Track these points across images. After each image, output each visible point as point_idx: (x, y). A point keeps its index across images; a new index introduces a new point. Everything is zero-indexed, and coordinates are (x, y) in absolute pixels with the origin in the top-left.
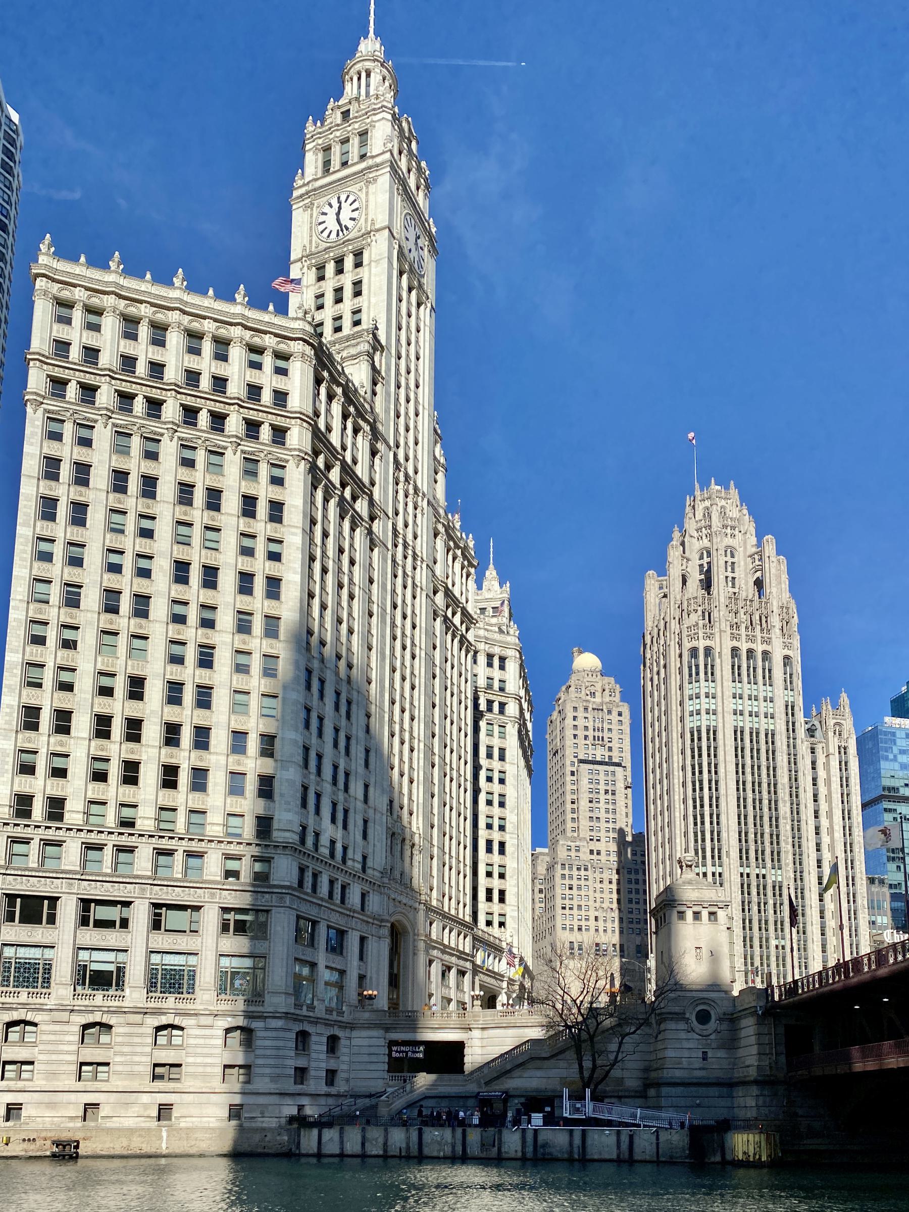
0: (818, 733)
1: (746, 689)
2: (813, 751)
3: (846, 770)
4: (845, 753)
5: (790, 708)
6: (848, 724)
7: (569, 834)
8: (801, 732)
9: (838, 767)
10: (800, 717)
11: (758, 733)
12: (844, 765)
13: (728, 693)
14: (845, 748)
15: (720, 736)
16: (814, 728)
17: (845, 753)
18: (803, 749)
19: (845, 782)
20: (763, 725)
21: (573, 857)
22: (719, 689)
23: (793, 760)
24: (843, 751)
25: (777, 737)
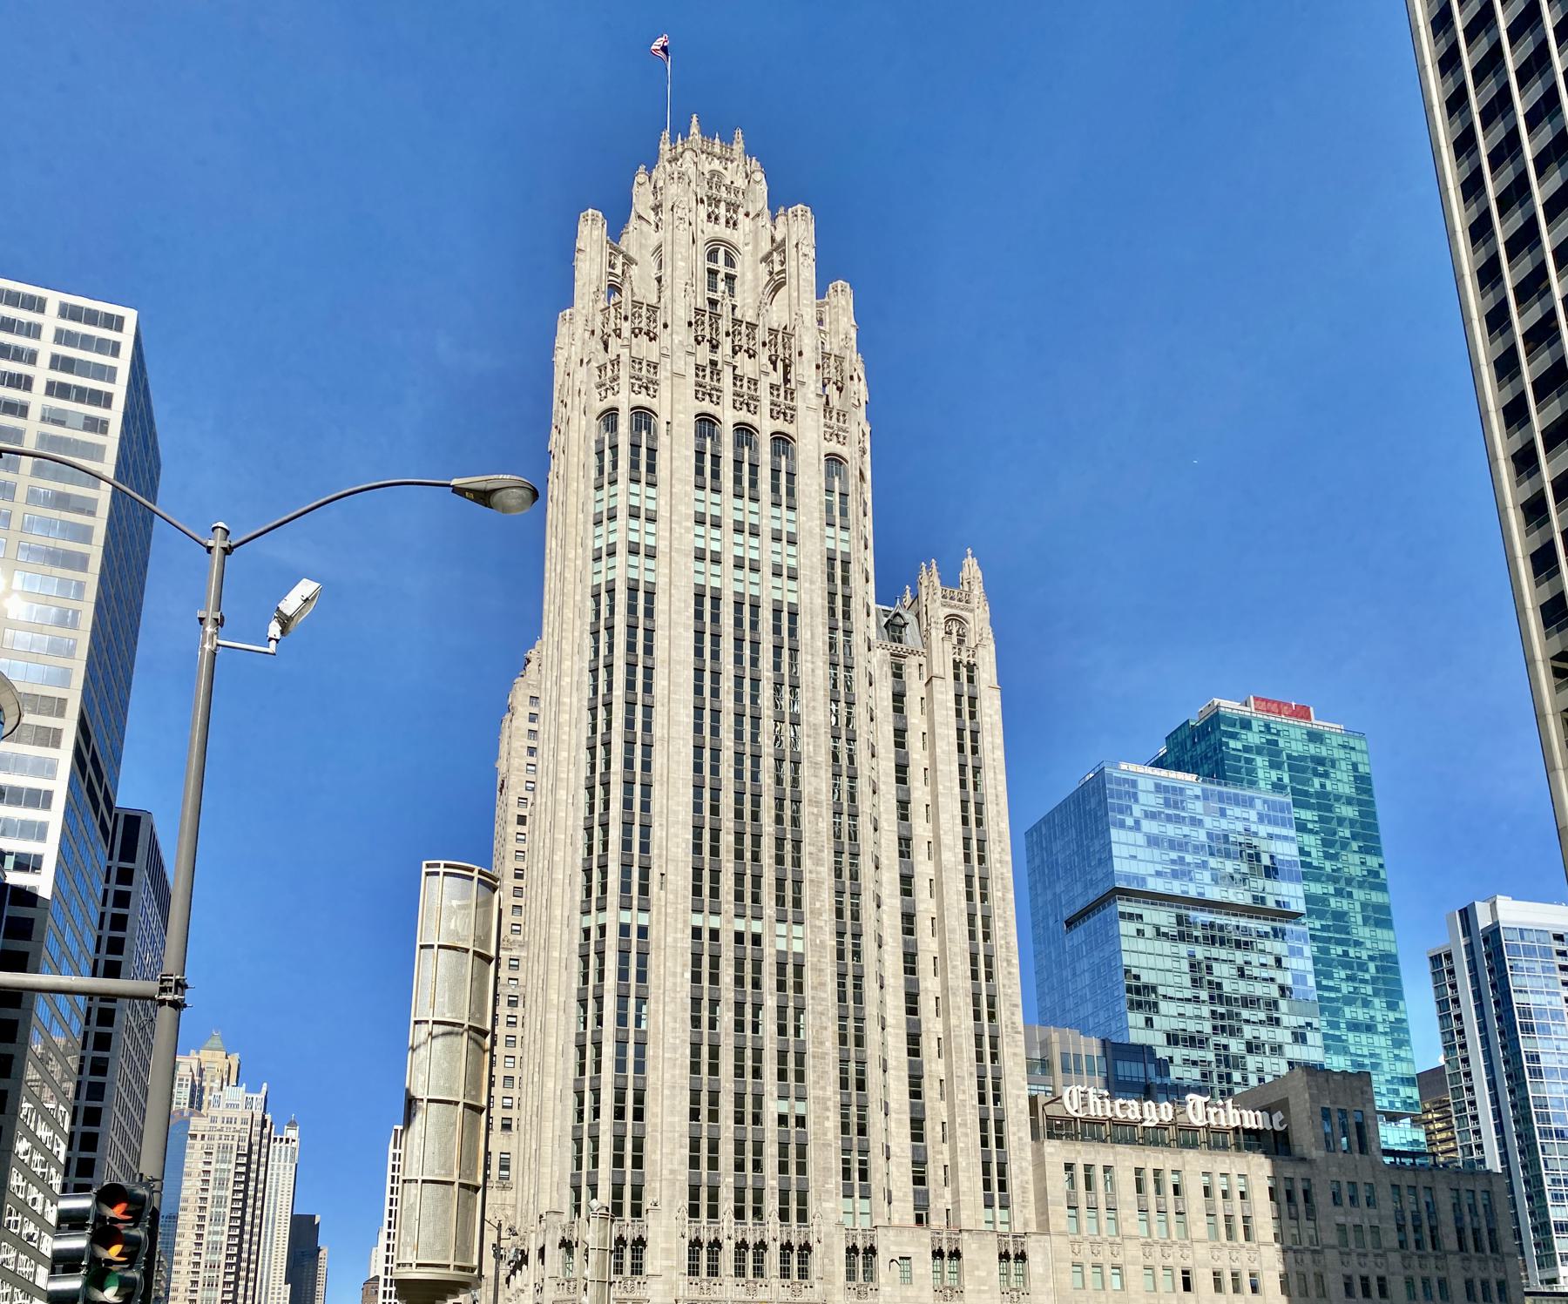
0: (911, 635)
1: (728, 507)
2: (898, 674)
3: (972, 715)
4: (971, 680)
5: (837, 566)
6: (979, 619)
8: (867, 625)
9: (952, 705)
10: (864, 591)
12: (967, 705)
13: (687, 510)
14: (971, 668)
15: (660, 604)
16: (898, 621)
18: (873, 661)
19: (968, 741)
20: (768, 590)
22: (663, 501)
24: (964, 672)
25: (802, 620)
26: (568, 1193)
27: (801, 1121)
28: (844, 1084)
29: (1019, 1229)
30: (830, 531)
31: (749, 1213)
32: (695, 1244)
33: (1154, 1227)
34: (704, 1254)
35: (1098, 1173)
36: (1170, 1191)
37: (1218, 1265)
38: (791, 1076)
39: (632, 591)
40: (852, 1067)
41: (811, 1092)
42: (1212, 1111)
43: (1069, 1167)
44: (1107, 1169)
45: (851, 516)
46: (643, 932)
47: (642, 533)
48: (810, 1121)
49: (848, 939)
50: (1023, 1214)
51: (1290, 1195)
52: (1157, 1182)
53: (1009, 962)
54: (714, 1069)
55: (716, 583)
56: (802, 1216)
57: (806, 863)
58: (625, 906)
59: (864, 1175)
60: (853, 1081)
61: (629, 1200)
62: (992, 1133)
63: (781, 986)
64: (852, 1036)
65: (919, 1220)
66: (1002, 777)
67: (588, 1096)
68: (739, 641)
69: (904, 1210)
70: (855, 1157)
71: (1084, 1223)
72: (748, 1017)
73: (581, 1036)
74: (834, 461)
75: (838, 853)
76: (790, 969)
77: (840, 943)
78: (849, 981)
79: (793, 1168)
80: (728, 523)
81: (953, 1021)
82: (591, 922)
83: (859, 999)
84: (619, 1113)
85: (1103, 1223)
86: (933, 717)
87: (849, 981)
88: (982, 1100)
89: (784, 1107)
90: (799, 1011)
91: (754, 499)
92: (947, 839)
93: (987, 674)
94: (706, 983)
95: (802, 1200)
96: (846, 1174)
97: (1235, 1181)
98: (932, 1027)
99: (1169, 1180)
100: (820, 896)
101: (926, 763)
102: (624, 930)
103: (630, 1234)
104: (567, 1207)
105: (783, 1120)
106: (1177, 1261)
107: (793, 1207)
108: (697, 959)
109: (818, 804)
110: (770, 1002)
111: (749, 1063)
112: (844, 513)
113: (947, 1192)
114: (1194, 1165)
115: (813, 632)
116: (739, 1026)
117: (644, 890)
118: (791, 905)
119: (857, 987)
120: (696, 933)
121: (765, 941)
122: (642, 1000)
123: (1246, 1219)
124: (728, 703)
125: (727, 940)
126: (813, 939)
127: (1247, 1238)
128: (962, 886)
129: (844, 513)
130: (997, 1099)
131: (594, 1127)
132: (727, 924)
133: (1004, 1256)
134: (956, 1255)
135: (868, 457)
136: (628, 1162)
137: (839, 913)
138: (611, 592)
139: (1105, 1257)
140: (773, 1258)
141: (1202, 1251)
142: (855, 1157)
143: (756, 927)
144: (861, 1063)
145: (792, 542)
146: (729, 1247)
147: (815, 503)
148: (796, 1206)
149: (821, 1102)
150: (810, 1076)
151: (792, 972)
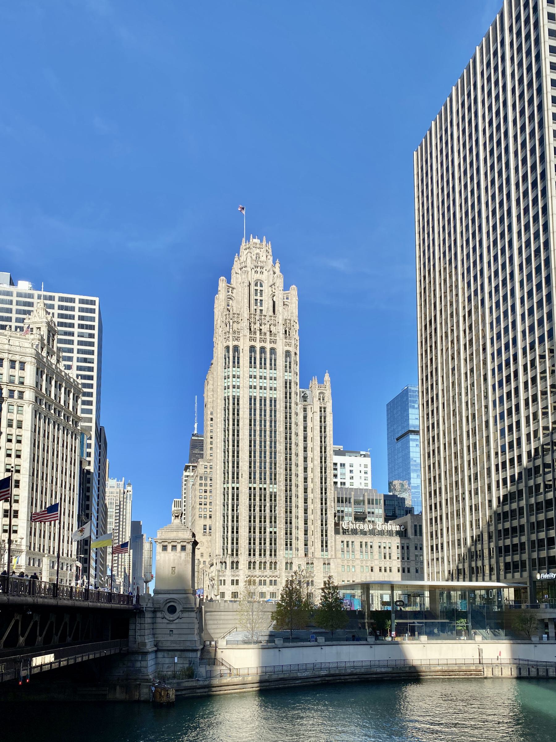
1: (258, 372)
2: (305, 410)
4: (325, 411)
5: (287, 384)
6: (328, 393)
7: (208, 457)
11: (265, 400)
12: (323, 419)
14: (325, 408)
15: (241, 402)
16: (306, 395)
17: (325, 411)
19: (323, 429)
20: (268, 394)
21: (208, 473)
23: (288, 417)
24: (323, 410)
26: (222, 550)
27: (275, 533)
28: (286, 523)
29: (329, 557)
30: (286, 374)
31: (263, 555)
32: (250, 562)
33: (364, 556)
34: (252, 564)
35: (350, 543)
36: (369, 547)
37: (380, 565)
38: (273, 522)
39: (234, 399)
40: (289, 519)
41: (277, 526)
42: (383, 526)
43: (342, 542)
44: (352, 542)
45: (292, 369)
46: (238, 488)
47: (236, 382)
48: (277, 533)
49: (288, 487)
50: (330, 553)
51: (403, 548)
52: (366, 545)
53: (331, 490)
54: (254, 521)
55: (255, 394)
56: (275, 555)
57: (278, 469)
58: (233, 482)
59: (291, 545)
60: (289, 522)
61: (235, 552)
62: (324, 533)
63: (271, 500)
64: (288, 511)
65: (306, 555)
66: (332, 439)
67: (226, 528)
68: (261, 410)
69: (302, 552)
70: (289, 540)
71: (345, 556)
72: (263, 508)
73: (224, 514)
74: (288, 354)
75: (286, 465)
76: (273, 496)
77: (286, 488)
78: (288, 498)
79: (273, 544)
80: (258, 377)
81: (315, 506)
82: (225, 486)
83: (291, 502)
84: (233, 532)
85: (351, 556)
86: (314, 423)
87: (288, 498)
88: (322, 525)
89: (271, 530)
90: (275, 506)
91: (265, 369)
92: (316, 458)
93: (329, 410)
94: (252, 501)
95: (275, 551)
96: (286, 545)
97: (387, 544)
98: (310, 507)
99: (369, 544)
100: (281, 478)
101: (312, 436)
102: (233, 488)
103: (235, 560)
104: (222, 554)
105: (271, 532)
106: (369, 564)
107: (273, 553)
108: (250, 496)
109: (280, 453)
110: (268, 505)
111: (263, 520)
112: (290, 367)
113: (313, 548)
114: (376, 541)
115: (280, 406)
116: (261, 511)
117: (238, 478)
118: (274, 479)
119: (291, 499)
120: (250, 488)
121: (267, 489)
122: (237, 506)
123: (390, 554)
124: (258, 428)
125: (257, 490)
126: (279, 488)
127: (390, 558)
128: (319, 470)
129: (290, 367)
130: (326, 525)
131: (227, 535)
132: (257, 486)
133: (324, 564)
134: (312, 563)
135: (298, 347)
136: (235, 543)
137: (286, 480)
138: (228, 399)
139: (350, 563)
140: (268, 565)
141: (377, 562)
142: (289, 540)
143: (265, 486)
144: (291, 518)
145: (275, 379)
146: (258, 563)
147: (281, 368)
148: (274, 552)
149: (280, 528)
150: (277, 522)
151: (273, 497)
